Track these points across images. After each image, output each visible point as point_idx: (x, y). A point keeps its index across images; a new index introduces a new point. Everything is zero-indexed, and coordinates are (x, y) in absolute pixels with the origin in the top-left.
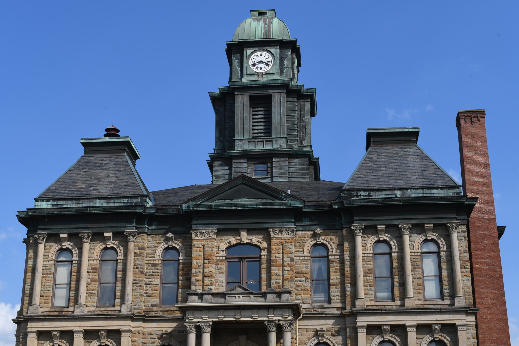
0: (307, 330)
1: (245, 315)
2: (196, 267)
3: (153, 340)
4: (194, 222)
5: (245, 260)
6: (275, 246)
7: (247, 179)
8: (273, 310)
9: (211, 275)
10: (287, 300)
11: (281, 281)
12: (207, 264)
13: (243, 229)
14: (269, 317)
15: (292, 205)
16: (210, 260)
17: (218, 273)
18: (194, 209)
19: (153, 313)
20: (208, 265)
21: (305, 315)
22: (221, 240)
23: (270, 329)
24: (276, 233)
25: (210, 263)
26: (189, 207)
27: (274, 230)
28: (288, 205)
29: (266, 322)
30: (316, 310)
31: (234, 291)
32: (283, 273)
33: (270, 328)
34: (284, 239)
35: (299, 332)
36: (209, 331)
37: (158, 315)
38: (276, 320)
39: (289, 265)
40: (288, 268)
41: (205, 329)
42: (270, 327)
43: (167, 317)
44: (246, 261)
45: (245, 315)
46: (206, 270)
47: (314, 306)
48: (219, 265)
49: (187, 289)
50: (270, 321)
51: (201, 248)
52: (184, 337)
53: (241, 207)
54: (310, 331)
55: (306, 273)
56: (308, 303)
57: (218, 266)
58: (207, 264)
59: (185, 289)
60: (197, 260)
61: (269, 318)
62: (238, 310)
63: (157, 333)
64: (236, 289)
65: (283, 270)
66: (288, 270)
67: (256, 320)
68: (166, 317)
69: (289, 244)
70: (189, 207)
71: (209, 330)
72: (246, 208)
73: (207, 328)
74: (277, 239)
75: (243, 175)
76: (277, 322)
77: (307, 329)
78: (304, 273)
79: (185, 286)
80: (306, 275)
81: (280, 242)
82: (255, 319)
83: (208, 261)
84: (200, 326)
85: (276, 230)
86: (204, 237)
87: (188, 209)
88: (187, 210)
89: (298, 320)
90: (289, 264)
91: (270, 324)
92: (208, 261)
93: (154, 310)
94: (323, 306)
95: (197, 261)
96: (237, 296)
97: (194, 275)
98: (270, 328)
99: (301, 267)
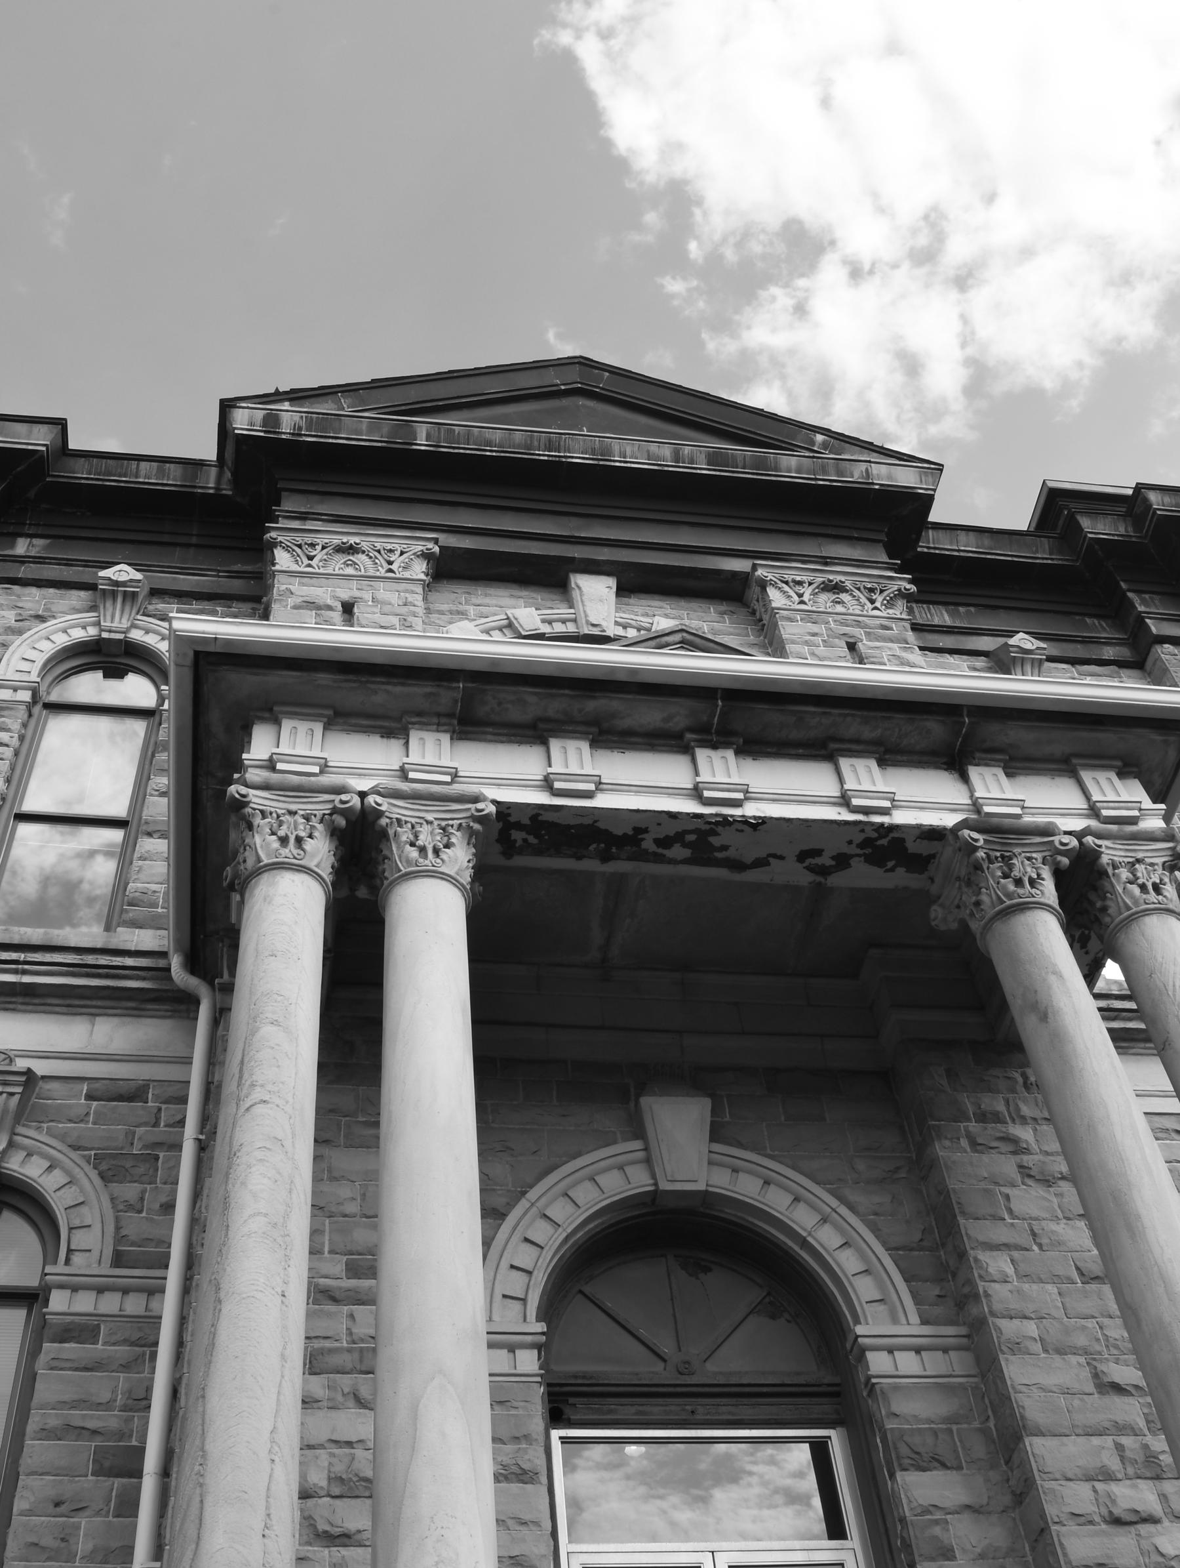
4: (289, 504)
6: (807, 643)
7: (607, 374)
13: (593, 568)
15: (879, 480)
18: (301, 435)
22: (451, 612)
24: (800, 595)
26: (272, 420)
27: (786, 583)
28: (853, 477)
34: (858, 624)
41: (422, 850)
43: (24, 972)
51: (330, 608)
52: (140, 1131)
53: (587, 456)
62: (715, 747)
67: (877, 819)
68: (16, 972)
69: (895, 646)
70: (272, 420)
72: (618, 464)
73: (447, 846)
74: (811, 616)
75: (582, 360)
81: (832, 634)
82: (867, 811)
84: (384, 821)
85: (800, 583)
86: (350, 571)
87: (265, 432)
88: (262, 434)
98: (1019, 882)
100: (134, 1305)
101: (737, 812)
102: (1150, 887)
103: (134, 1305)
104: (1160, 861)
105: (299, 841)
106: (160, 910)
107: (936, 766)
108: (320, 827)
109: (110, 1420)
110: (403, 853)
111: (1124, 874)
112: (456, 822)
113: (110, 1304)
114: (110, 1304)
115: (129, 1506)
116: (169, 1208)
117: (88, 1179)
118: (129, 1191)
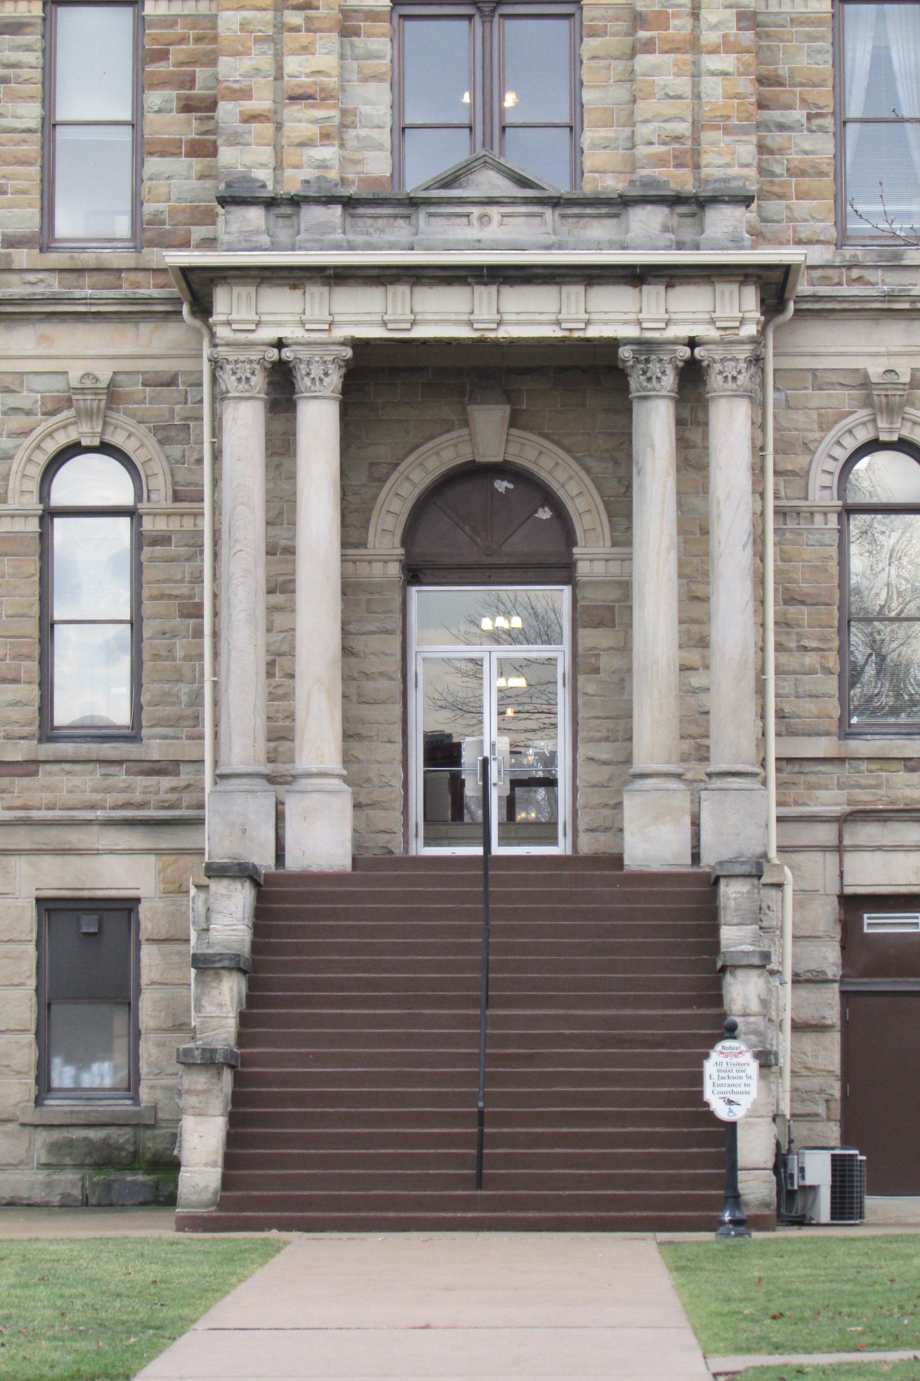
0: (815, 376)
1: (518, 313)
2: (240, 47)
3: (17, 422)
5: (493, 11)
8: (662, 288)
9: (323, 90)
10: (736, 243)
11: (684, 128)
12: (295, 29)
14: (645, 325)
16: (317, 8)
17: (355, 77)
19: (14, 278)
20: (303, 37)
21: (807, 302)
23: (645, 384)
25: (317, 25)
29: (625, 353)
30: (859, 280)
31: (461, 186)
32: (695, 85)
33: (649, 379)
35: (776, 389)
36: (333, 392)
37: (40, 290)
38: (675, 342)
39: (727, 46)
40: (725, 62)
42: (649, 374)
43: (91, 304)
44: (501, 16)
45: (518, 313)
46: (292, 64)
47: (855, 256)
48: (358, 35)
49: (187, 156)
50: (645, 347)
52: (178, 407)
54: (832, 384)
55: (815, 85)
56: (818, 242)
57: (354, 39)
58: (295, 29)
59: (179, 155)
60: (243, 8)
61: (642, 329)
62: (486, 284)
63: (39, 383)
64: (472, 177)
65: (696, 76)
66: (724, 74)
67: (576, 335)
68: (86, 304)
71: (335, 380)
76: (685, 352)
77: (817, 373)
78: (802, 85)
79: (181, 140)
80: (812, 94)
83: (307, 17)
89: (775, 332)
90: (732, 39)
91: (647, 361)
92: (303, 14)
93: (16, 266)
94: (898, 256)
95: (245, 14)
96: (476, 211)
97: (234, 91)
98: (649, 379)
99: (785, 52)
100: (188, 523)
101: (492, 335)
102: (730, 379)
103: (188, 523)
104: (742, 356)
105: (248, 379)
106: (167, 227)
107: (626, 284)
108: (257, 367)
109: (184, 590)
110: (303, 383)
111: (717, 367)
112: (331, 358)
113: (174, 524)
114: (174, 524)
115: (198, 633)
116: (200, 461)
117: (151, 441)
118: (175, 451)
